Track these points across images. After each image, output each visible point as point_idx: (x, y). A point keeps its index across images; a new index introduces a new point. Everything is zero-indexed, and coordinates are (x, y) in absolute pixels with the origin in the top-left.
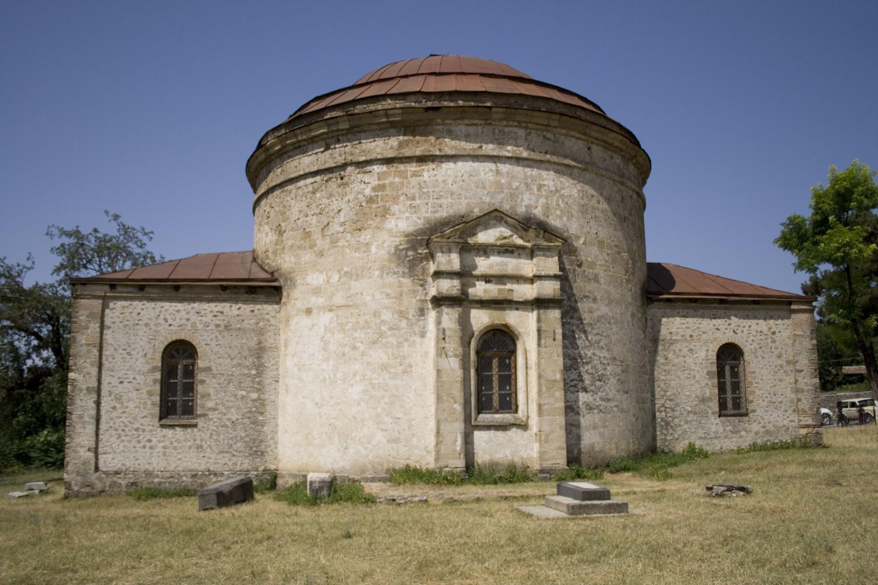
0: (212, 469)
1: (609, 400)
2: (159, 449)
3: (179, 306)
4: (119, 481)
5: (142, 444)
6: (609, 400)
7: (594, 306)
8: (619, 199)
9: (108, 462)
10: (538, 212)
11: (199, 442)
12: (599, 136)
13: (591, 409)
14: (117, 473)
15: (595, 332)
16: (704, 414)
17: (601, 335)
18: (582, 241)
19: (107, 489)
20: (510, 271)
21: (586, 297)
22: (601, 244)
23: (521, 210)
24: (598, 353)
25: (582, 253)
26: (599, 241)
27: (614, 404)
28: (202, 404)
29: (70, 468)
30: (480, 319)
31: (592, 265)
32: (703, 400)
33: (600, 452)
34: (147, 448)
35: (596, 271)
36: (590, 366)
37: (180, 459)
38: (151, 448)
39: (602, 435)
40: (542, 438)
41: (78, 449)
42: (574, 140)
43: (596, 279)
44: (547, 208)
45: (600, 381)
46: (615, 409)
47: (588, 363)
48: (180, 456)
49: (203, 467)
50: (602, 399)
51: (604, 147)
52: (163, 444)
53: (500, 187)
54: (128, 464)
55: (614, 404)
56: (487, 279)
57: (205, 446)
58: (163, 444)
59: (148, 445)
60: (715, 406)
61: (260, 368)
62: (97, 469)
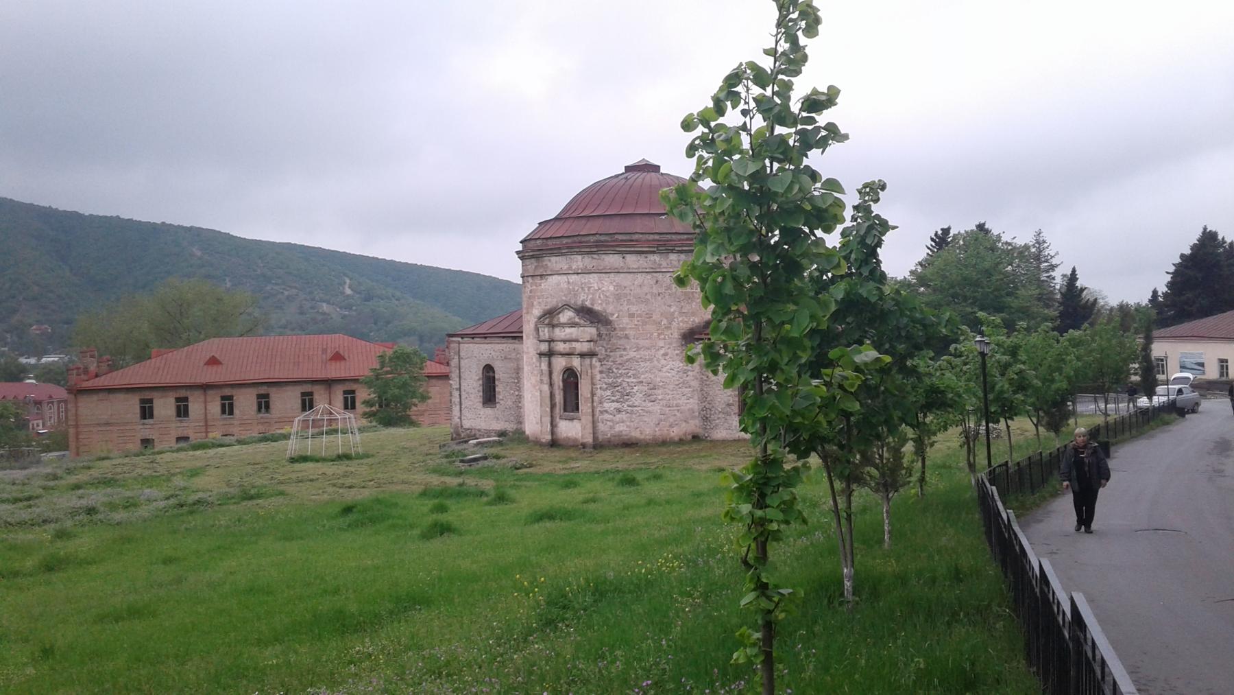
3: (486, 346)
9: (467, 424)
10: (588, 304)
16: (728, 414)
20: (574, 336)
23: (579, 303)
28: (499, 397)
30: (560, 363)
31: (623, 329)
32: (729, 405)
40: (584, 428)
43: (627, 337)
44: (593, 300)
53: (570, 292)
56: (564, 341)
60: (736, 409)
61: (519, 379)
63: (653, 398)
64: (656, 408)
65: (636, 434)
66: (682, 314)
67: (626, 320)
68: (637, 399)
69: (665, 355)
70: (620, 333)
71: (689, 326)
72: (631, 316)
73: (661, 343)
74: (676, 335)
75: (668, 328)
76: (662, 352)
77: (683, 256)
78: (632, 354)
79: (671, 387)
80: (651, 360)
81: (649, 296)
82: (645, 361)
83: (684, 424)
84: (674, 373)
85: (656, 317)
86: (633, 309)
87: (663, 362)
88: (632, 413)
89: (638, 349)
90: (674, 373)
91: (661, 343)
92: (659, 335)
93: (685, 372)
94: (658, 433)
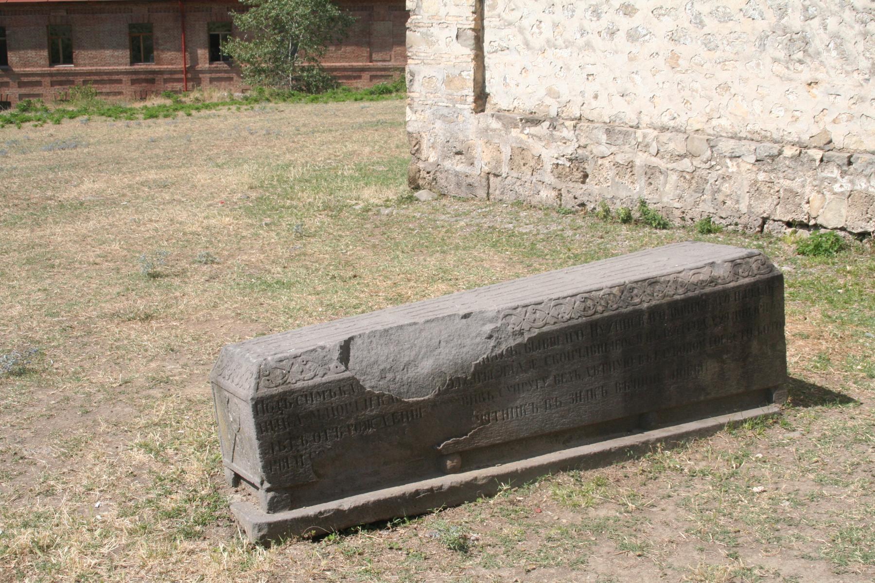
0: (838, 141)
2: (659, 43)
4: (537, 148)
5: (604, 22)
11: (794, 20)
14: (532, 120)
19: (504, 170)
29: (417, 90)
34: (621, 35)
37: (724, 87)
38: (633, 36)
41: (435, 30)
48: (723, 76)
49: (804, 129)
52: (668, 24)
54: (564, 90)
57: (819, 40)
58: (668, 24)
59: (624, 23)
62: (481, 98)
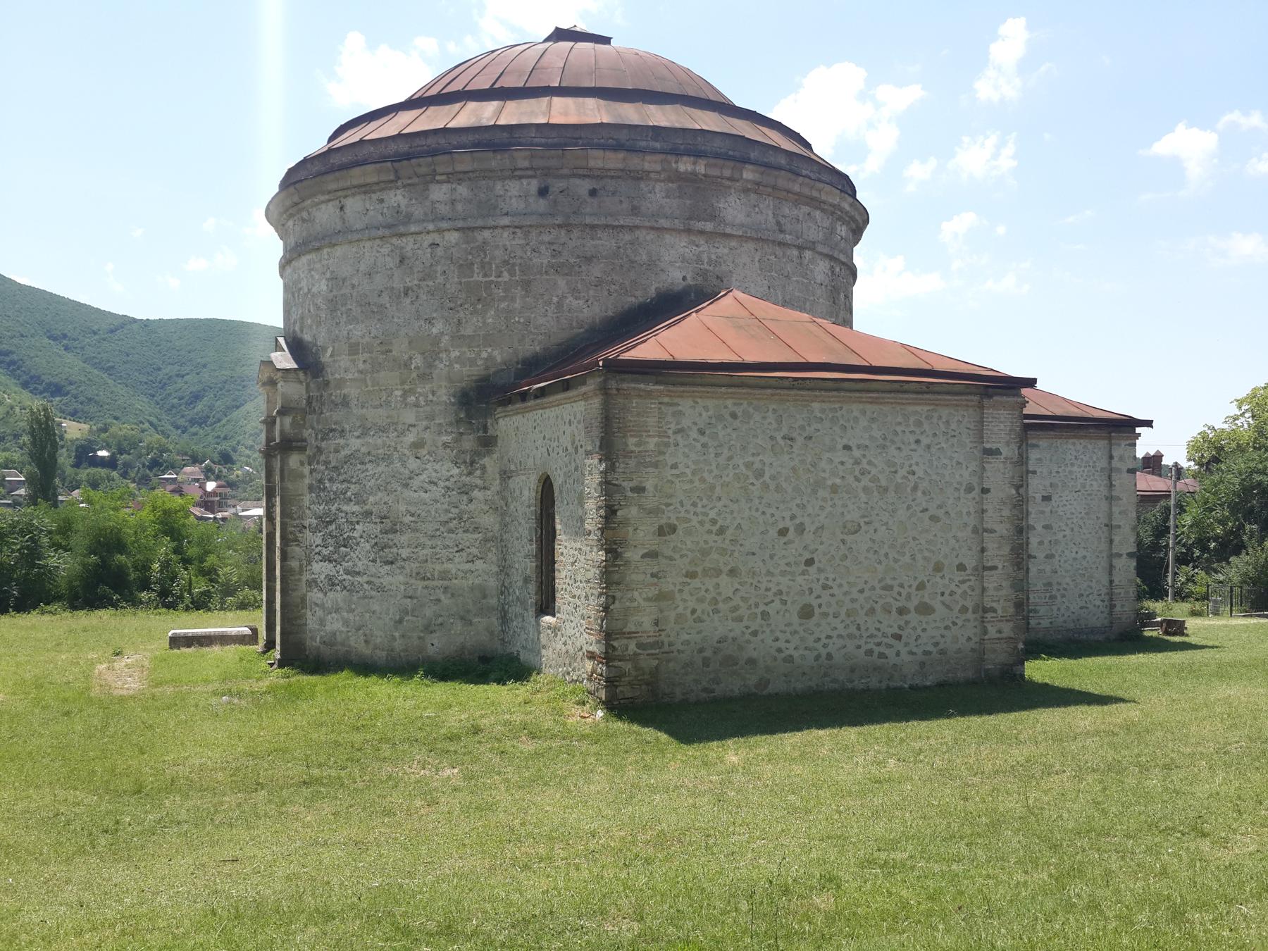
1: (358, 573)
6: (358, 573)
7: (342, 441)
8: (391, 262)
12: (342, 184)
13: (333, 584)
15: (341, 478)
17: (349, 482)
18: (330, 351)
21: (332, 430)
22: (354, 349)
24: (345, 508)
25: (329, 370)
26: (351, 346)
27: (365, 578)
31: (341, 383)
33: (343, 644)
35: (345, 391)
36: (334, 526)
39: (346, 623)
42: (323, 206)
43: (345, 403)
45: (345, 546)
46: (366, 586)
47: (330, 523)
50: (347, 572)
51: (365, 193)
55: (365, 578)
63: (389, 553)
64: (394, 580)
65: (357, 644)
66: (458, 338)
67: (344, 361)
68: (360, 557)
69: (418, 445)
70: (337, 394)
71: (477, 370)
72: (354, 349)
73: (409, 416)
74: (444, 395)
75: (424, 377)
76: (411, 438)
77: (463, 190)
78: (355, 443)
79: (430, 527)
80: (387, 458)
81: (385, 299)
82: (376, 460)
83: (459, 626)
84: (436, 492)
85: (400, 349)
86: (358, 331)
87: (413, 464)
88: (350, 589)
89: (364, 434)
90: (436, 492)
91: (409, 416)
92: (405, 394)
93: (465, 490)
94: (398, 645)
